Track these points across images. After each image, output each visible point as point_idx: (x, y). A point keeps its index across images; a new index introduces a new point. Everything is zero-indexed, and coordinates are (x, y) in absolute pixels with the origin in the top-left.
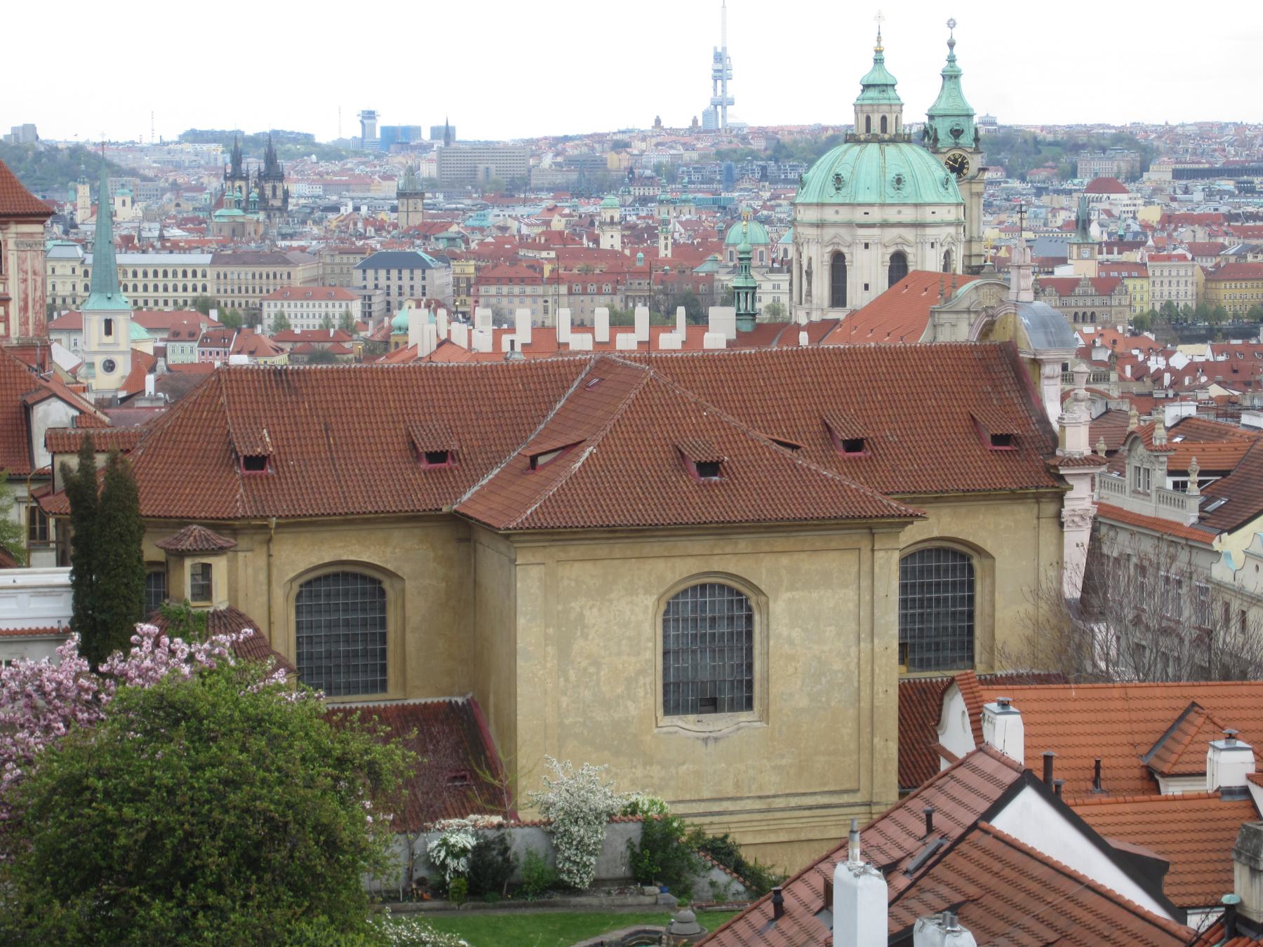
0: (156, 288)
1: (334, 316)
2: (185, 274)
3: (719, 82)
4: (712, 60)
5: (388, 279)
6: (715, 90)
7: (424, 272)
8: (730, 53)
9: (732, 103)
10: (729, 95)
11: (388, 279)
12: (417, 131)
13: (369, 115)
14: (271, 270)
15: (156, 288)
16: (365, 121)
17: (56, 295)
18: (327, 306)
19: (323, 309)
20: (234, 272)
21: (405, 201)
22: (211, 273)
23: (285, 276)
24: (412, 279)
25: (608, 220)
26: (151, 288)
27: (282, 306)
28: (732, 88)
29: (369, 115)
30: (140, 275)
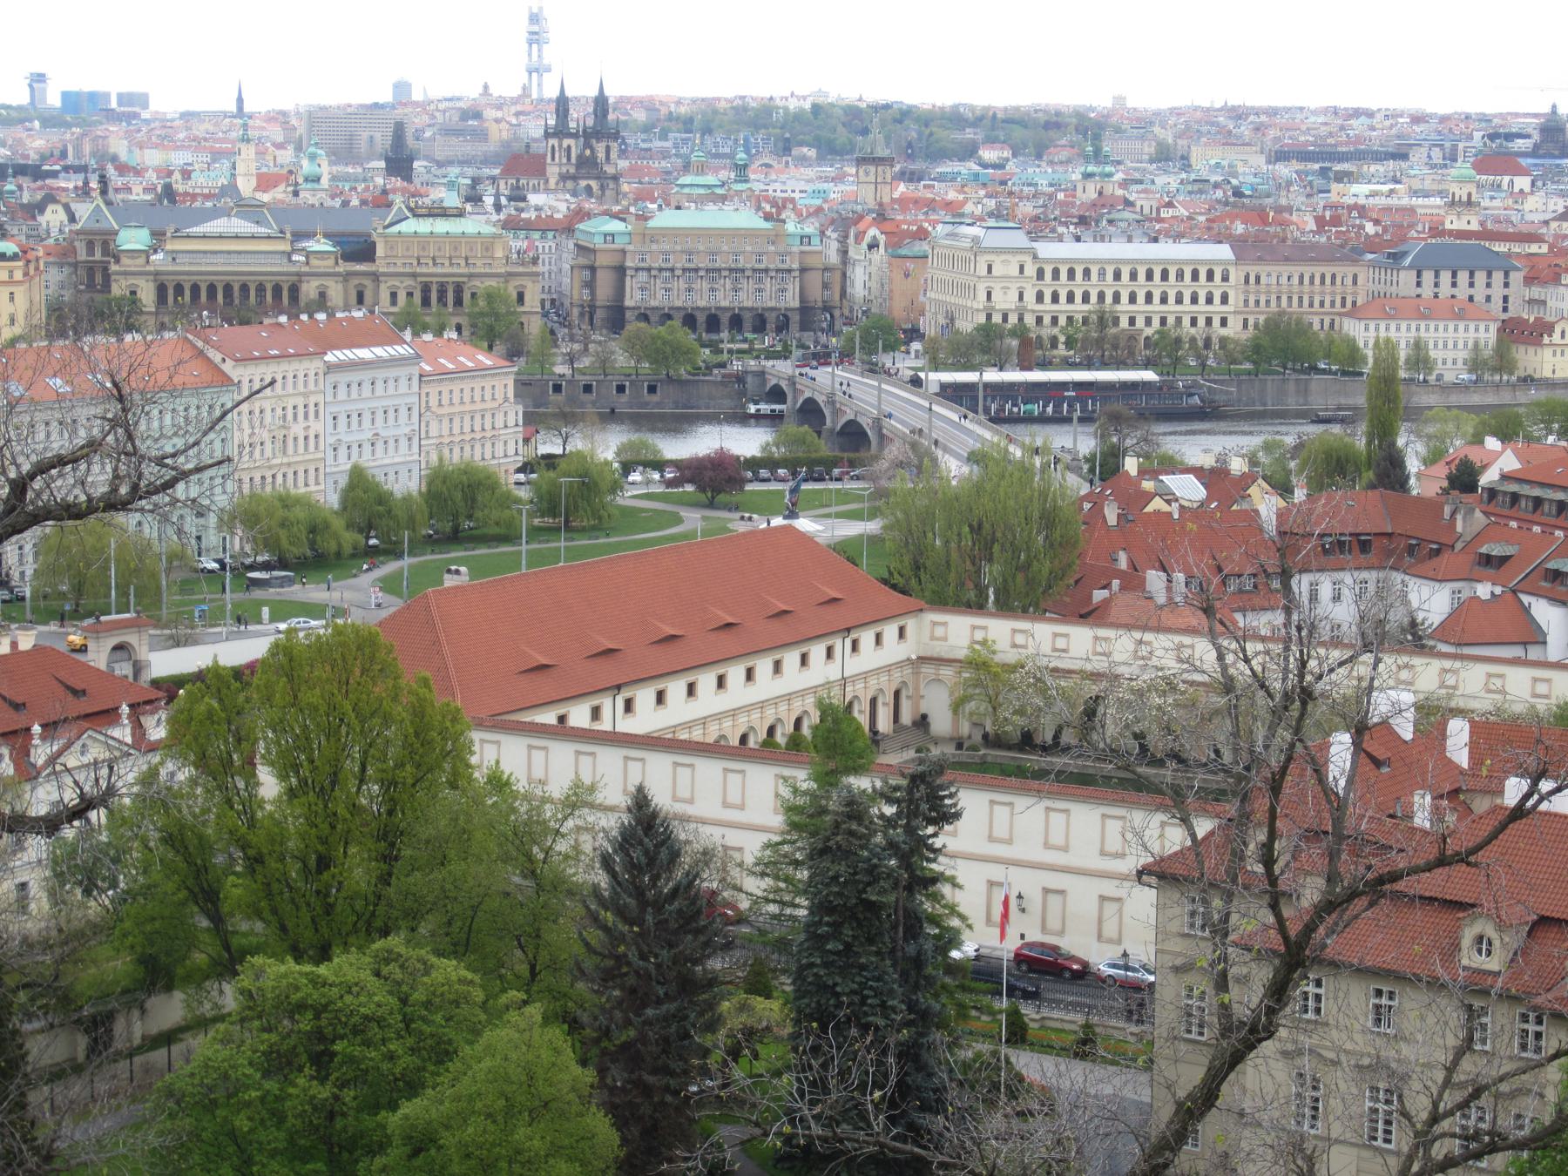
0: (1149, 298)
1: (1366, 345)
2: (1195, 276)
3: (535, 47)
4: (526, 21)
5: (1454, 285)
6: (530, 55)
7: (1506, 275)
8: (546, 13)
9: (548, 70)
10: (545, 62)
11: (1454, 285)
12: (107, 96)
13: (39, 78)
14: (1328, 270)
15: (1149, 298)
16: (35, 85)
17: (993, 308)
18: (1477, 330)
19: (1472, 334)
20: (1271, 274)
21: (872, 169)
22: (1236, 275)
23: (1349, 281)
24: (1488, 285)
25: (1465, 198)
26: (1141, 298)
27: (1418, 329)
28: (550, 54)
29: (39, 78)
30: (1125, 276)
